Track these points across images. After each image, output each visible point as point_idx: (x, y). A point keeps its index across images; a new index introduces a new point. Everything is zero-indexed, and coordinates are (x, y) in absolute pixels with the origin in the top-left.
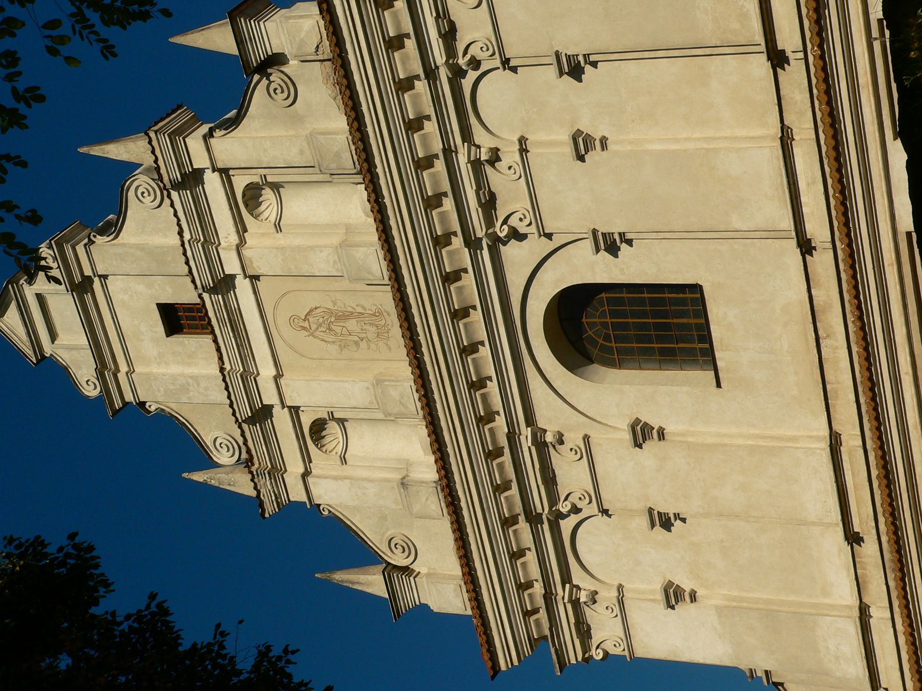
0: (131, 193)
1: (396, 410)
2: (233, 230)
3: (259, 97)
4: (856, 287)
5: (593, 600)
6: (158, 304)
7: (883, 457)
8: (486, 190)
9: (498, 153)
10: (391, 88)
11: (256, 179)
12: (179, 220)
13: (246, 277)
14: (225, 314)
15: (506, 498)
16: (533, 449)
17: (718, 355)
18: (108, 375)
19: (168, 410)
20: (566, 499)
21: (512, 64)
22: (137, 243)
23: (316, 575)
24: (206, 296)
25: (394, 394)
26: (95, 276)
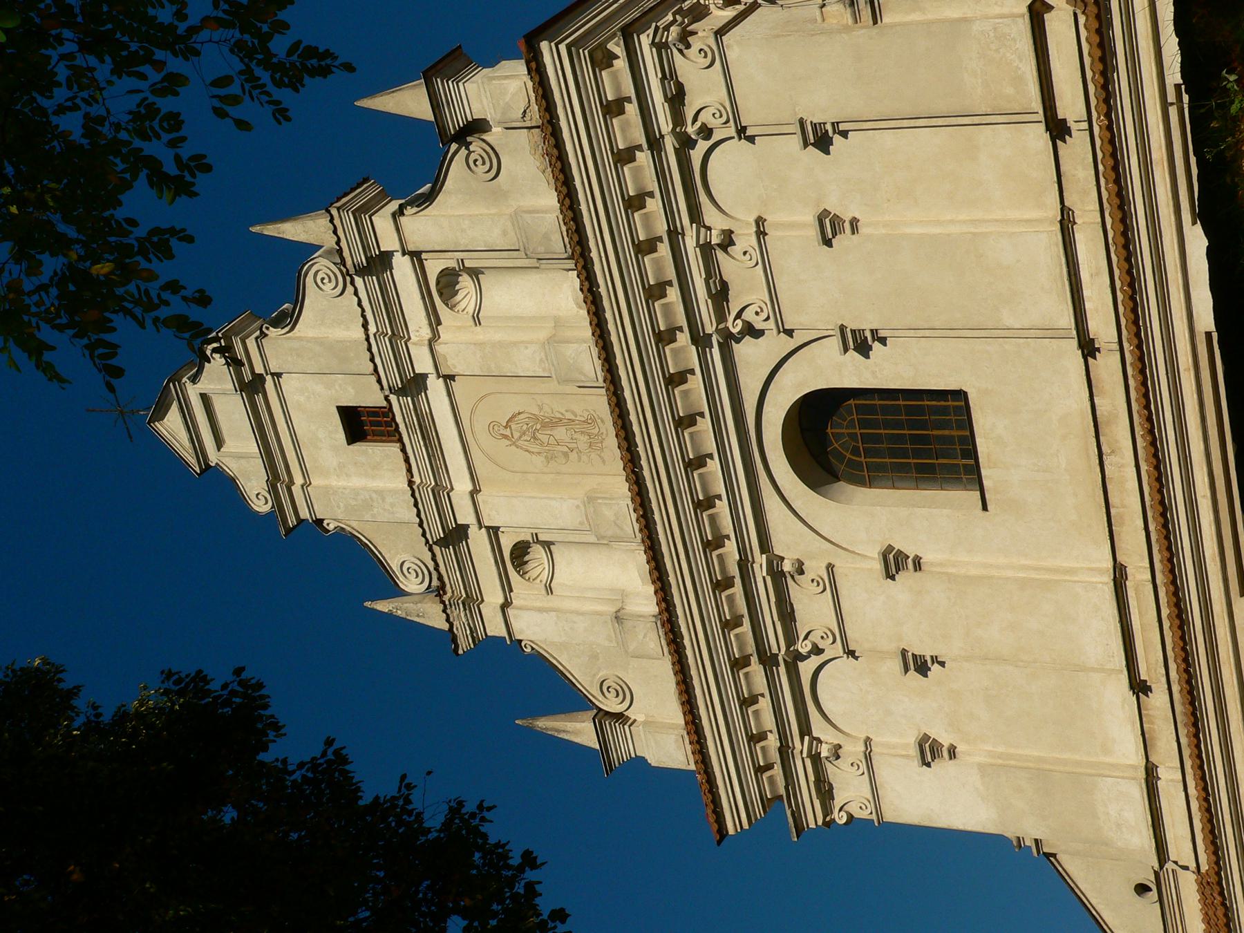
0: (310, 279)
1: (610, 533)
2: (425, 322)
3: (457, 169)
4: (1146, 395)
5: (836, 755)
6: (338, 408)
7: (1176, 594)
8: (717, 278)
9: (732, 235)
10: (608, 159)
11: (453, 264)
12: (363, 311)
13: (439, 376)
14: (415, 419)
15: (737, 636)
16: (769, 579)
17: (984, 472)
19: (348, 529)
20: (806, 638)
21: (749, 132)
22: (316, 336)
23: (517, 722)
24: (393, 398)
25: (608, 513)
26: (267, 374)
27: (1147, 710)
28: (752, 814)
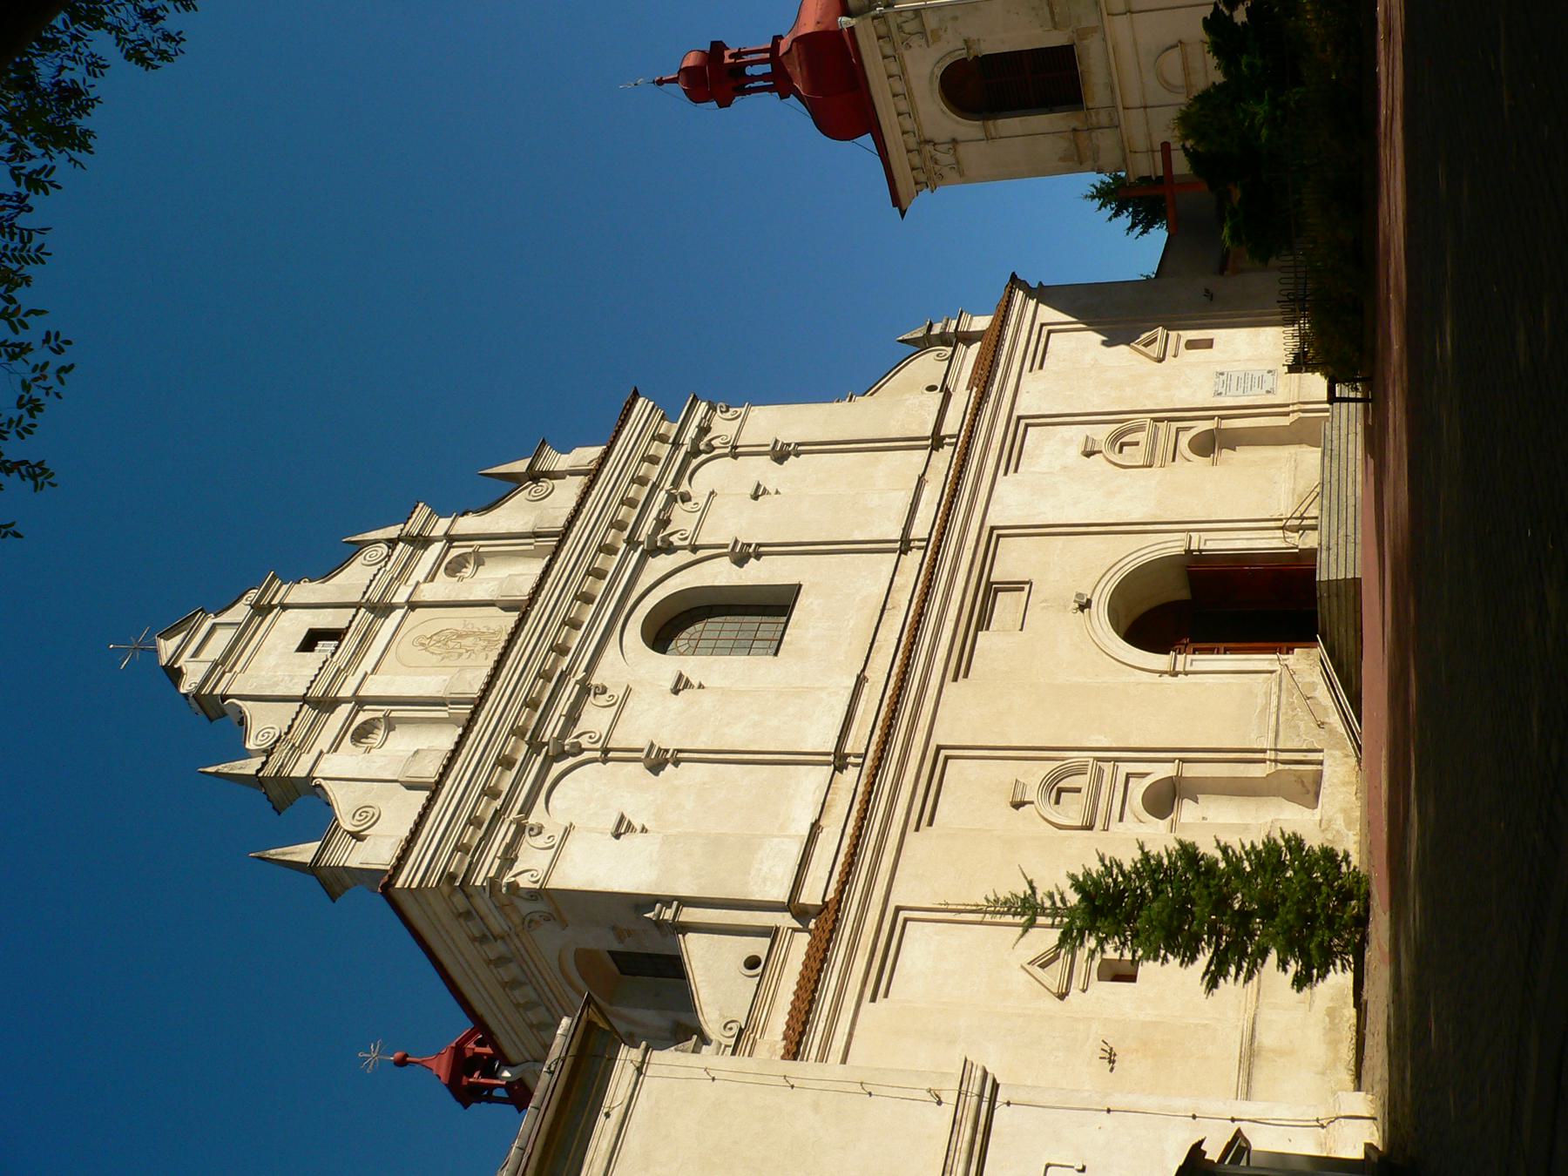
27: (835, 783)
28: (427, 879)
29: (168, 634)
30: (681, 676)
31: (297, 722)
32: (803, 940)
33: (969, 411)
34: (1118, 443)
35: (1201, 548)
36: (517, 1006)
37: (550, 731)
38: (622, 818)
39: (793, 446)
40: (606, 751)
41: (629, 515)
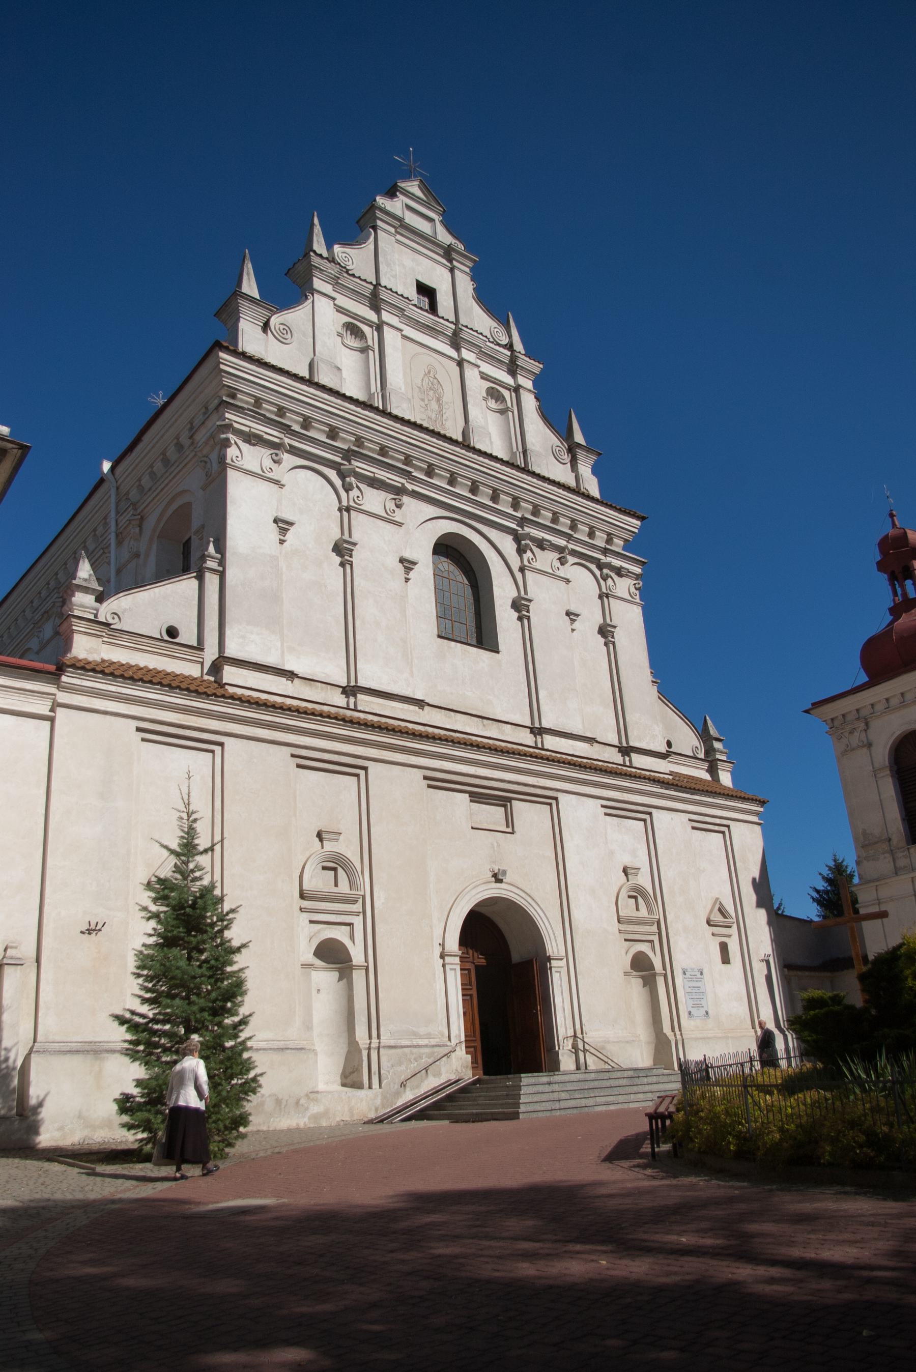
4: (536, 757)
18: (397, 223)
23: (247, 250)
28: (229, 376)
29: (423, 187)
30: (415, 563)
31: (358, 280)
32: (192, 670)
33: (652, 774)
34: (636, 894)
35: (553, 969)
36: (151, 466)
37: (359, 465)
38: (291, 524)
39: (612, 640)
40: (348, 509)
41: (545, 518)
